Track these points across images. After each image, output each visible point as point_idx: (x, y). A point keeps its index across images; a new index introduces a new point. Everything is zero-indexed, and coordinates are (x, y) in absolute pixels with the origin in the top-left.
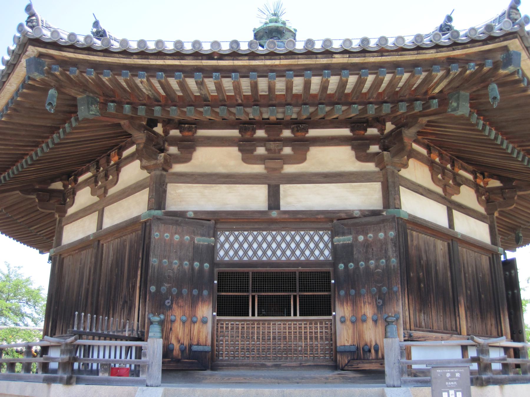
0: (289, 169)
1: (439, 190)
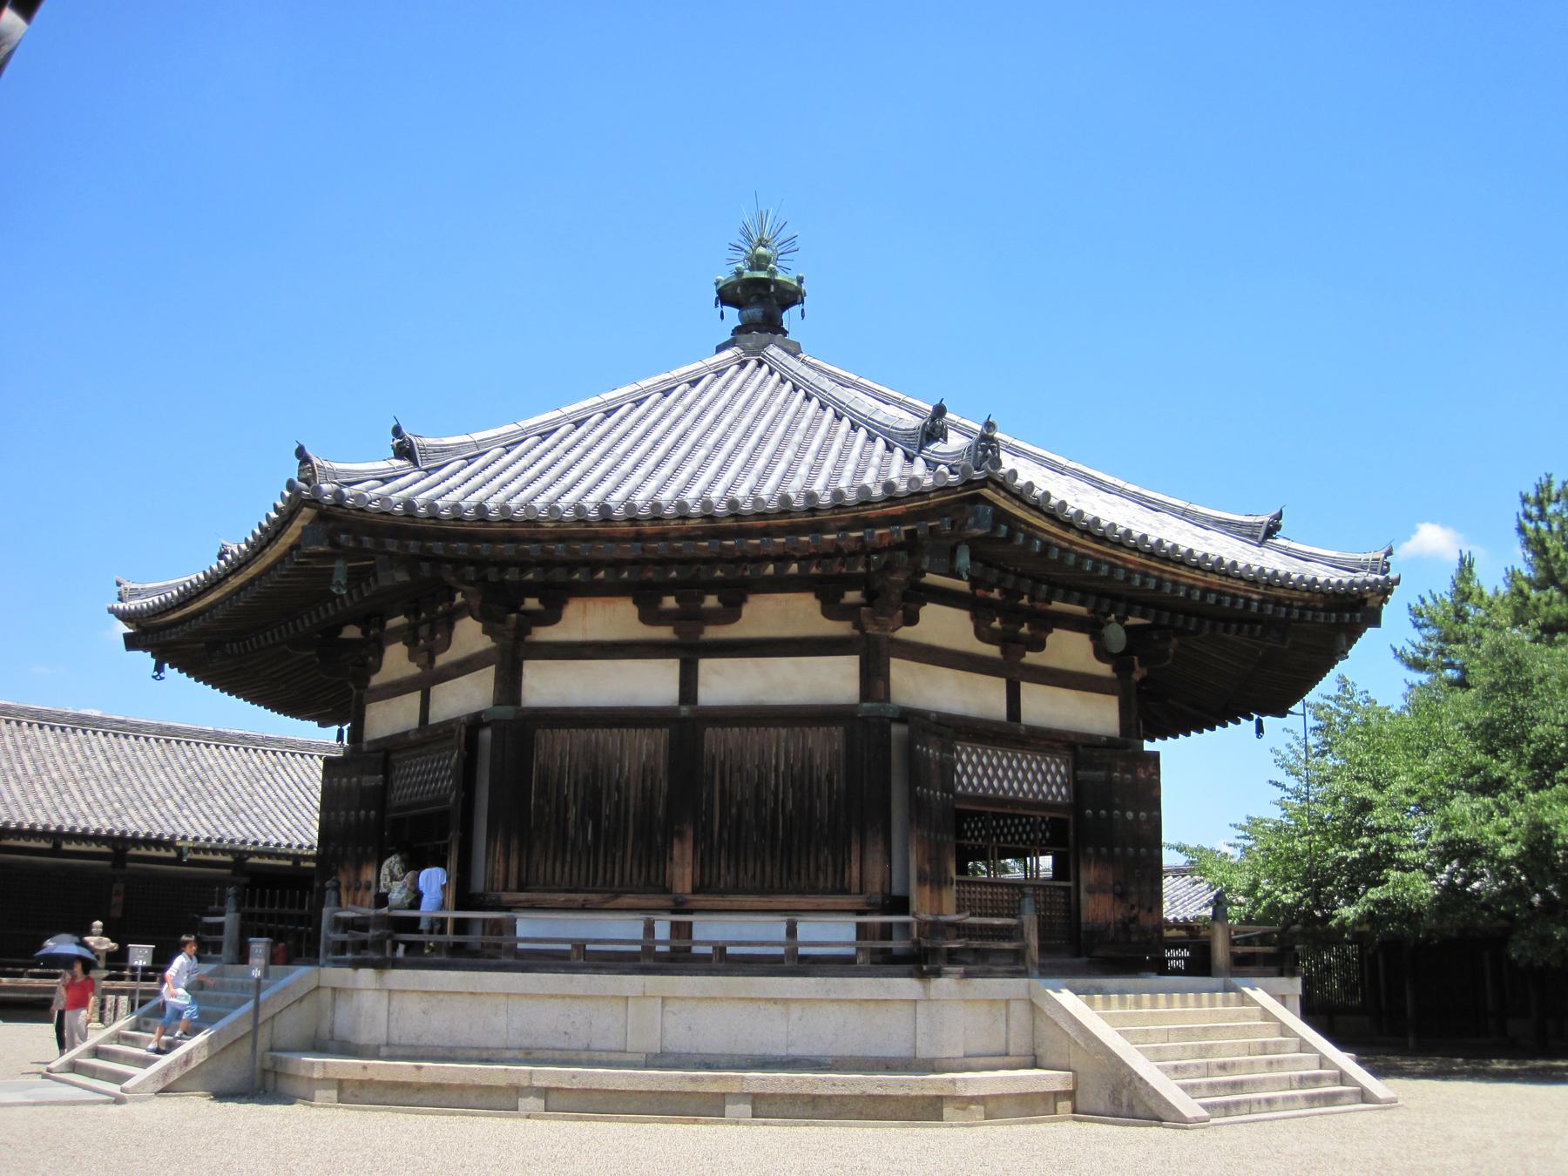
0: (713, 633)
1: (993, 651)
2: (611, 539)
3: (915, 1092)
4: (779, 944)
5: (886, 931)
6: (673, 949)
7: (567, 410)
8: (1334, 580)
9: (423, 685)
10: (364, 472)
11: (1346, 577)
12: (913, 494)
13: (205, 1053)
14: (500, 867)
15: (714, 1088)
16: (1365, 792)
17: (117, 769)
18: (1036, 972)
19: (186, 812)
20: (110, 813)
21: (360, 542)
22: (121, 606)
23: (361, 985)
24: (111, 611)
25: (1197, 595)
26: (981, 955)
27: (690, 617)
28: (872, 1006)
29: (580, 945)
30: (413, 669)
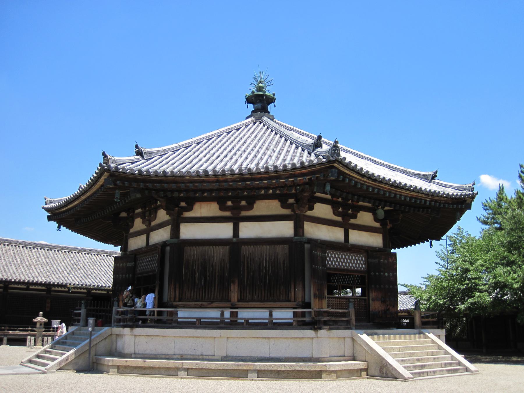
0: (244, 213)
1: (339, 219)
2: (209, 182)
3: (313, 369)
4: (267, 319)
5: (303, 314)
6: (231, 321)
7: (194, 139)
8: (455, 194)
9: (147, 232)
10: (126, 160)
11: (459, 193)
12: (310, 166)
13: (73, 357)
14: (173, 294)
15: (244, 368)
16: (467, 266)
17: (48, 261)
18: (354, 328)
19: (71, 275)
20: (46, 276)
21: (124, 184)
22: (46, 206)
23: (125, 333)
24: (43, 208)
25: (408, 199)
26: (335, 322)
27: (236, 208)
28: (298, 340)
29: (199, 319)
30: (144, 227)
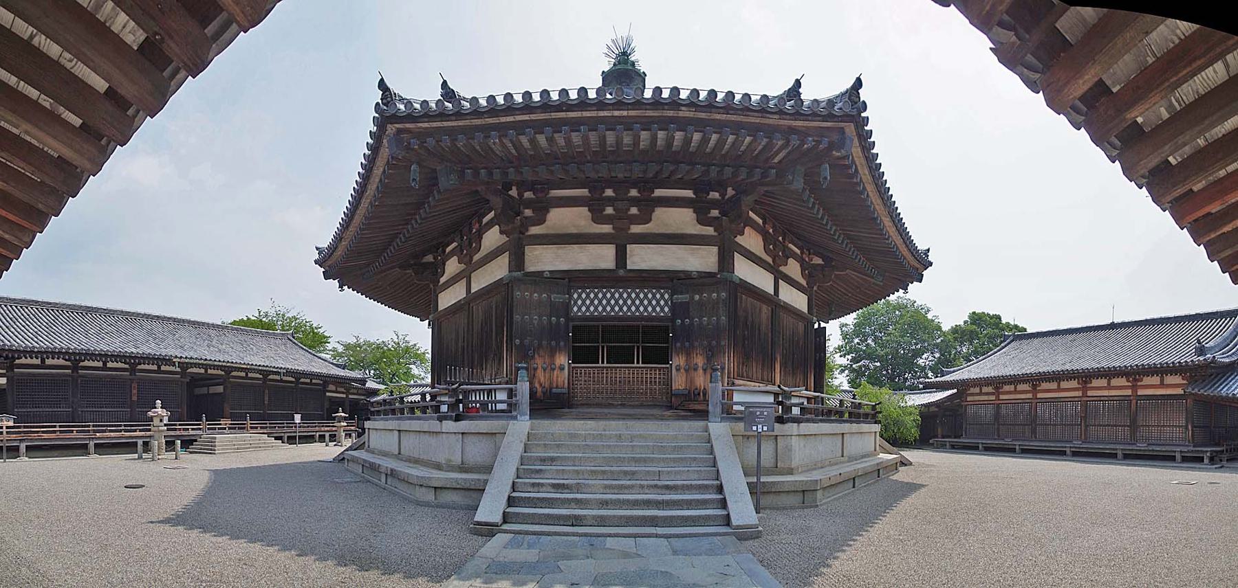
0: (636, 229)
27: (622, 220)
